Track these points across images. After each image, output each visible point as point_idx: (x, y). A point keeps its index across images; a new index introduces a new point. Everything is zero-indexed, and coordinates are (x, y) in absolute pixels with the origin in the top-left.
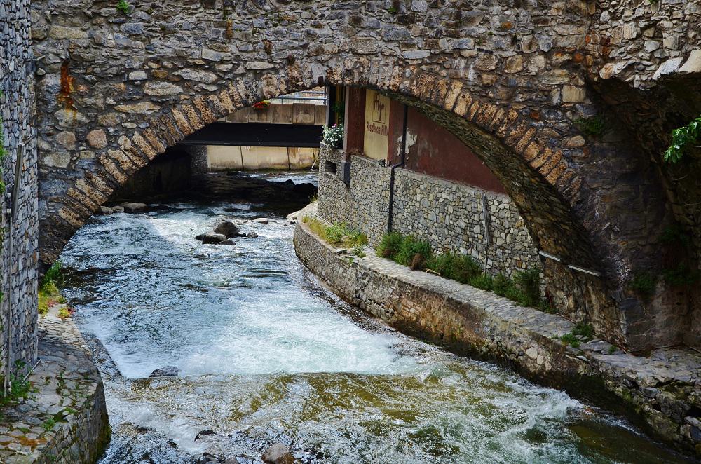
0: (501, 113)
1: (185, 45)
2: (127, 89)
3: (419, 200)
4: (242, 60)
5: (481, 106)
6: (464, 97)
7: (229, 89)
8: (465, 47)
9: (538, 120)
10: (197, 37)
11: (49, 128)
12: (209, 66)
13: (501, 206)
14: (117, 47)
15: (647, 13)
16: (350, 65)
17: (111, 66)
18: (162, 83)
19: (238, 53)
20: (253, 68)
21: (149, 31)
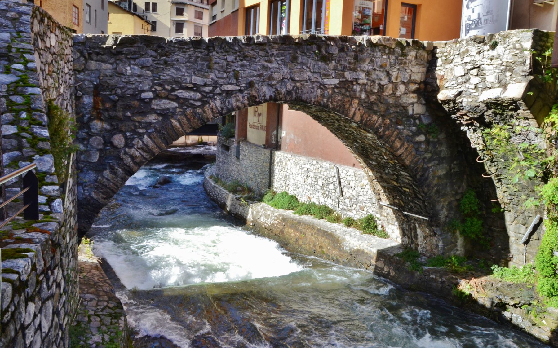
0: (380, 120)
1: (180, 73)
2: (140, 105)
3: (289, 168)
4: (219, 84)
5: (369, 116)
6: (359, 110)
7: (210, 104)
8: (360, 77)
9: (400, 125)
10: (189, 68)
11: (84, 134)
12: (196, 88)
13: (349, 174)
14: (132, 75)
16: (290, 87)
17: (129, 89)
18: (164, 101)
19: (216, 79)
20: (226, 89)
21: (156, 64)
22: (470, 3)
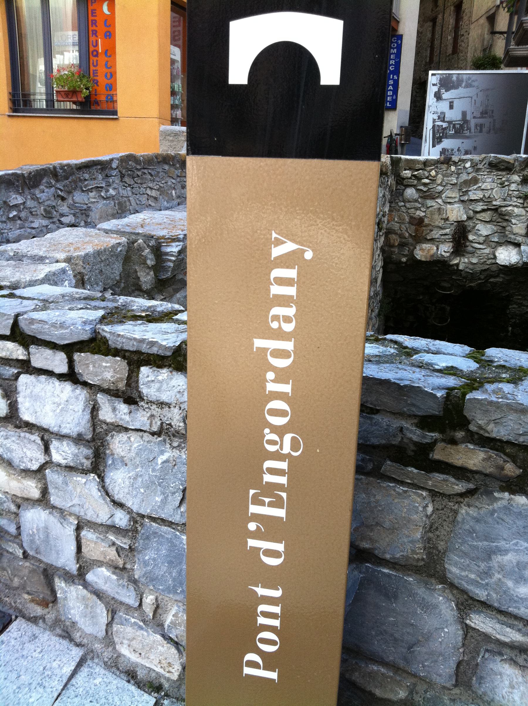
15: (489, 197)
22: (443, 91)
